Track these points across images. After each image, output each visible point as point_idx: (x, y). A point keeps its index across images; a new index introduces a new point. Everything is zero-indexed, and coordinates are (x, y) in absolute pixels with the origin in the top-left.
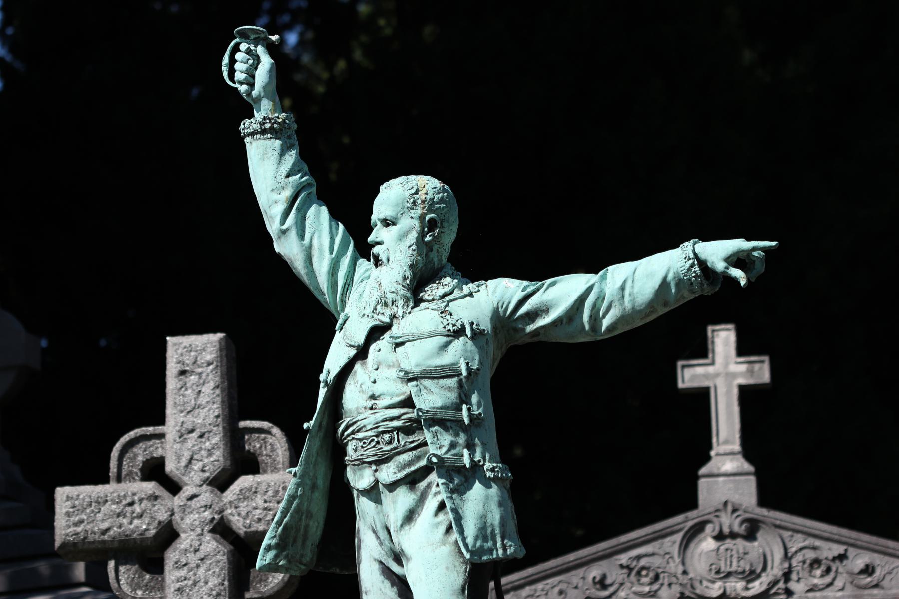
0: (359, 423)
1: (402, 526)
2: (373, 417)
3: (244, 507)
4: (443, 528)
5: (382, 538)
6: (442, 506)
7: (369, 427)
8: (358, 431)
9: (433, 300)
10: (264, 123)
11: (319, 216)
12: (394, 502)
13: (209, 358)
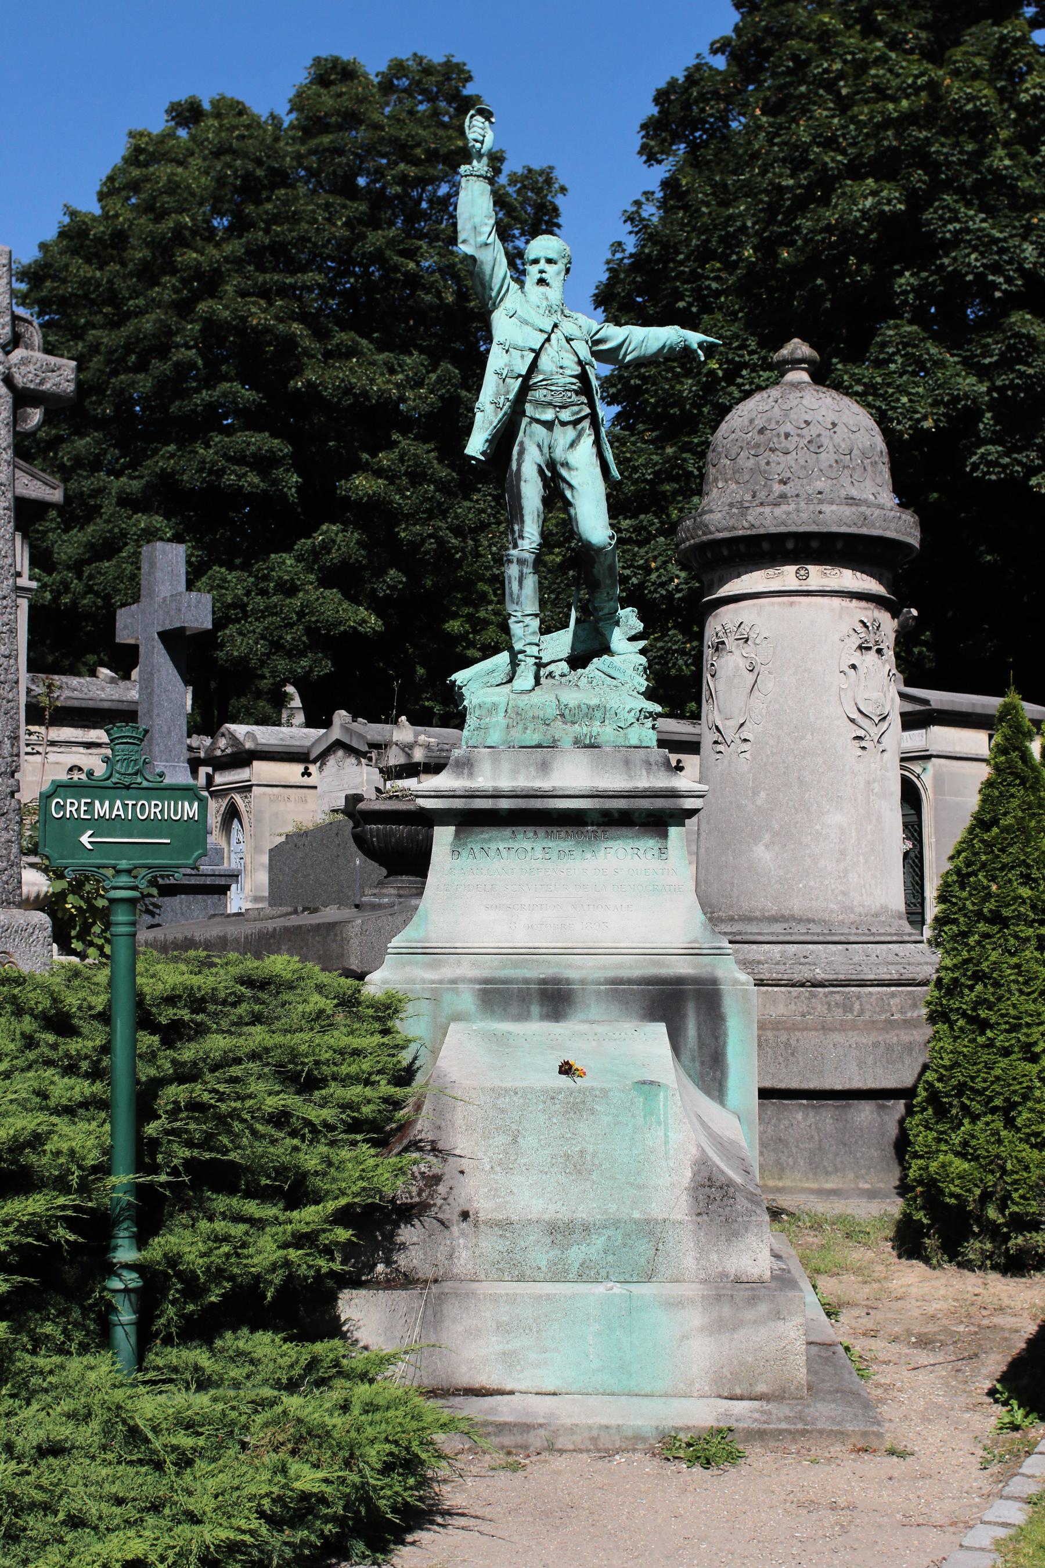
3: (24, 369)
12: (565, 433)
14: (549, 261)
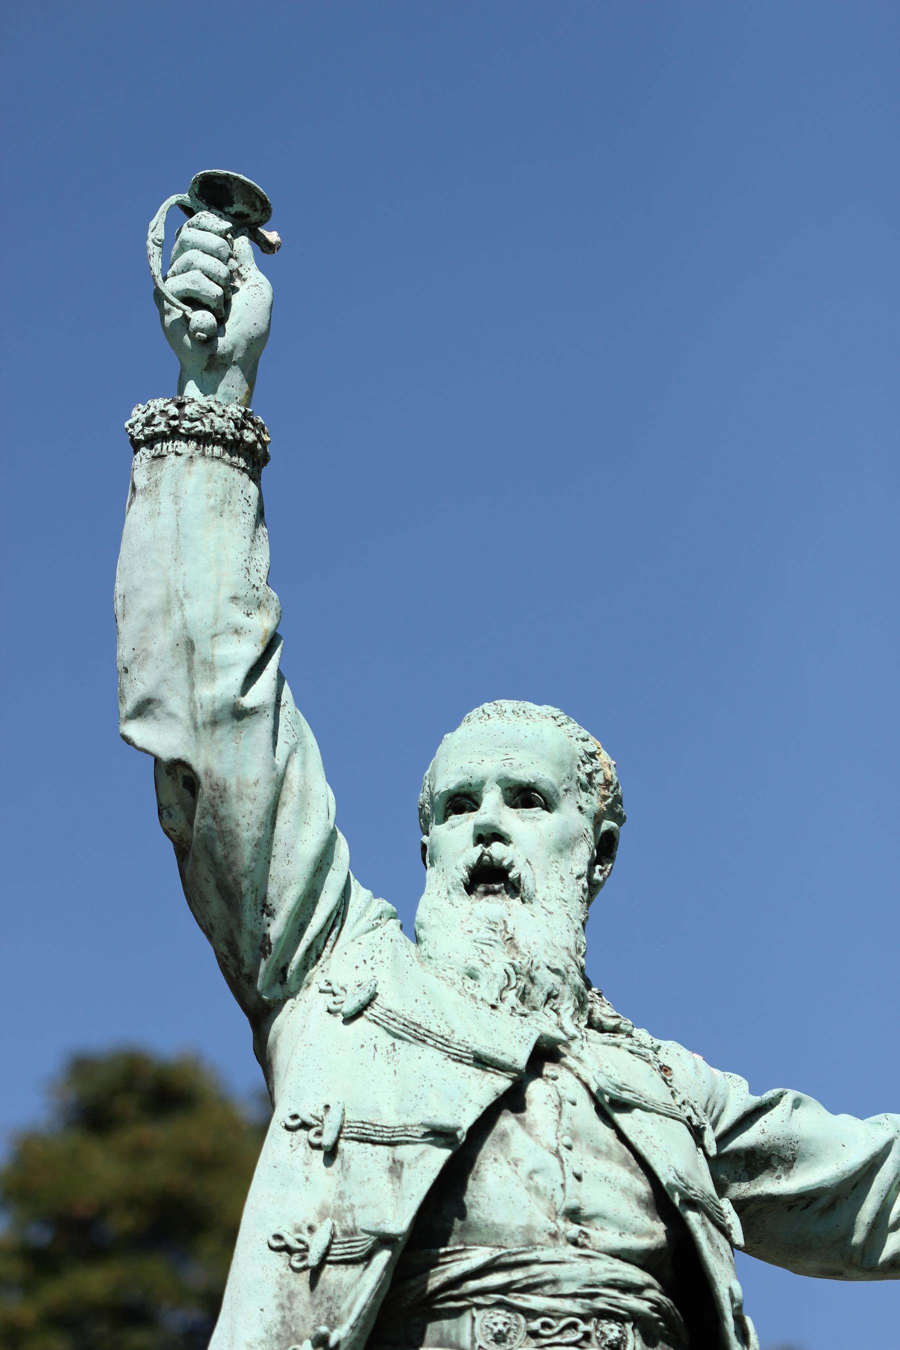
0: (536, 1269)
2: (583, 1262)
8: (528, 1289)
10: (243, 427)
14: (523, 796)
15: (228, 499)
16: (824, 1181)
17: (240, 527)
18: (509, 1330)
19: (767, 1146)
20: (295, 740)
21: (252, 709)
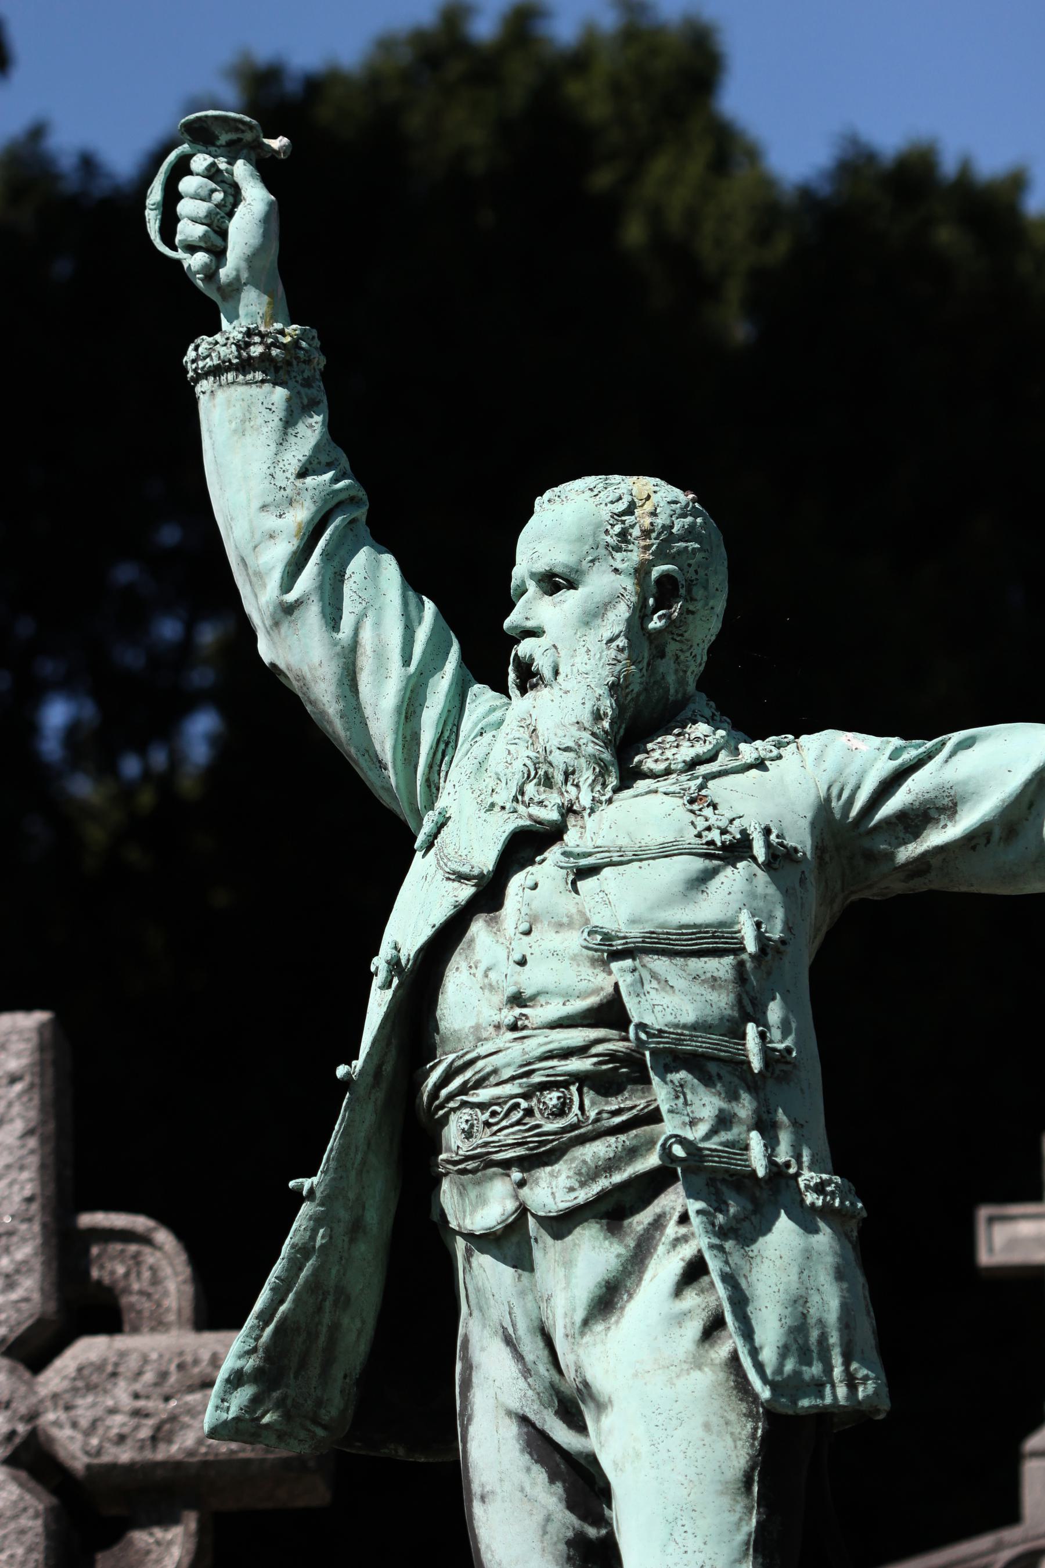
0: (480, 1064)
1: (586, 1323)
2: (518, 1047)
3: (85, 1408)
4: (694, 1328)
5: (529, 1358)
6: (694, 1272)
7: (506, 1074)
8: (479, 1084)
9: (668, 772)
10: (248, 345)
11: (376, 579)
12: (568, 1264)
13: (14, 1064)
15: (248, 415)
16: (985, 815)
17: (263, 438)
18: (472, 1126)
19: (917, 803)
20: (360, 607)
21: (296, 601)
